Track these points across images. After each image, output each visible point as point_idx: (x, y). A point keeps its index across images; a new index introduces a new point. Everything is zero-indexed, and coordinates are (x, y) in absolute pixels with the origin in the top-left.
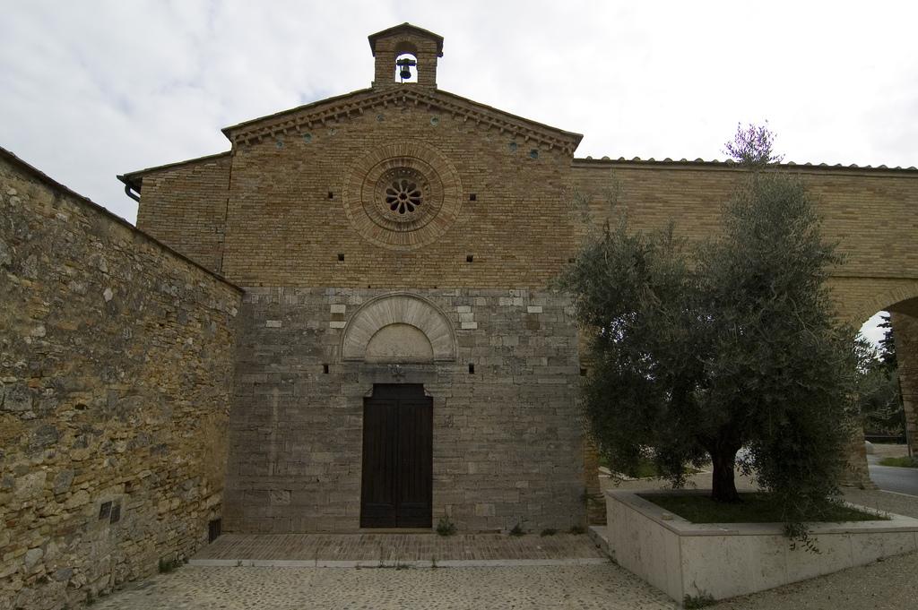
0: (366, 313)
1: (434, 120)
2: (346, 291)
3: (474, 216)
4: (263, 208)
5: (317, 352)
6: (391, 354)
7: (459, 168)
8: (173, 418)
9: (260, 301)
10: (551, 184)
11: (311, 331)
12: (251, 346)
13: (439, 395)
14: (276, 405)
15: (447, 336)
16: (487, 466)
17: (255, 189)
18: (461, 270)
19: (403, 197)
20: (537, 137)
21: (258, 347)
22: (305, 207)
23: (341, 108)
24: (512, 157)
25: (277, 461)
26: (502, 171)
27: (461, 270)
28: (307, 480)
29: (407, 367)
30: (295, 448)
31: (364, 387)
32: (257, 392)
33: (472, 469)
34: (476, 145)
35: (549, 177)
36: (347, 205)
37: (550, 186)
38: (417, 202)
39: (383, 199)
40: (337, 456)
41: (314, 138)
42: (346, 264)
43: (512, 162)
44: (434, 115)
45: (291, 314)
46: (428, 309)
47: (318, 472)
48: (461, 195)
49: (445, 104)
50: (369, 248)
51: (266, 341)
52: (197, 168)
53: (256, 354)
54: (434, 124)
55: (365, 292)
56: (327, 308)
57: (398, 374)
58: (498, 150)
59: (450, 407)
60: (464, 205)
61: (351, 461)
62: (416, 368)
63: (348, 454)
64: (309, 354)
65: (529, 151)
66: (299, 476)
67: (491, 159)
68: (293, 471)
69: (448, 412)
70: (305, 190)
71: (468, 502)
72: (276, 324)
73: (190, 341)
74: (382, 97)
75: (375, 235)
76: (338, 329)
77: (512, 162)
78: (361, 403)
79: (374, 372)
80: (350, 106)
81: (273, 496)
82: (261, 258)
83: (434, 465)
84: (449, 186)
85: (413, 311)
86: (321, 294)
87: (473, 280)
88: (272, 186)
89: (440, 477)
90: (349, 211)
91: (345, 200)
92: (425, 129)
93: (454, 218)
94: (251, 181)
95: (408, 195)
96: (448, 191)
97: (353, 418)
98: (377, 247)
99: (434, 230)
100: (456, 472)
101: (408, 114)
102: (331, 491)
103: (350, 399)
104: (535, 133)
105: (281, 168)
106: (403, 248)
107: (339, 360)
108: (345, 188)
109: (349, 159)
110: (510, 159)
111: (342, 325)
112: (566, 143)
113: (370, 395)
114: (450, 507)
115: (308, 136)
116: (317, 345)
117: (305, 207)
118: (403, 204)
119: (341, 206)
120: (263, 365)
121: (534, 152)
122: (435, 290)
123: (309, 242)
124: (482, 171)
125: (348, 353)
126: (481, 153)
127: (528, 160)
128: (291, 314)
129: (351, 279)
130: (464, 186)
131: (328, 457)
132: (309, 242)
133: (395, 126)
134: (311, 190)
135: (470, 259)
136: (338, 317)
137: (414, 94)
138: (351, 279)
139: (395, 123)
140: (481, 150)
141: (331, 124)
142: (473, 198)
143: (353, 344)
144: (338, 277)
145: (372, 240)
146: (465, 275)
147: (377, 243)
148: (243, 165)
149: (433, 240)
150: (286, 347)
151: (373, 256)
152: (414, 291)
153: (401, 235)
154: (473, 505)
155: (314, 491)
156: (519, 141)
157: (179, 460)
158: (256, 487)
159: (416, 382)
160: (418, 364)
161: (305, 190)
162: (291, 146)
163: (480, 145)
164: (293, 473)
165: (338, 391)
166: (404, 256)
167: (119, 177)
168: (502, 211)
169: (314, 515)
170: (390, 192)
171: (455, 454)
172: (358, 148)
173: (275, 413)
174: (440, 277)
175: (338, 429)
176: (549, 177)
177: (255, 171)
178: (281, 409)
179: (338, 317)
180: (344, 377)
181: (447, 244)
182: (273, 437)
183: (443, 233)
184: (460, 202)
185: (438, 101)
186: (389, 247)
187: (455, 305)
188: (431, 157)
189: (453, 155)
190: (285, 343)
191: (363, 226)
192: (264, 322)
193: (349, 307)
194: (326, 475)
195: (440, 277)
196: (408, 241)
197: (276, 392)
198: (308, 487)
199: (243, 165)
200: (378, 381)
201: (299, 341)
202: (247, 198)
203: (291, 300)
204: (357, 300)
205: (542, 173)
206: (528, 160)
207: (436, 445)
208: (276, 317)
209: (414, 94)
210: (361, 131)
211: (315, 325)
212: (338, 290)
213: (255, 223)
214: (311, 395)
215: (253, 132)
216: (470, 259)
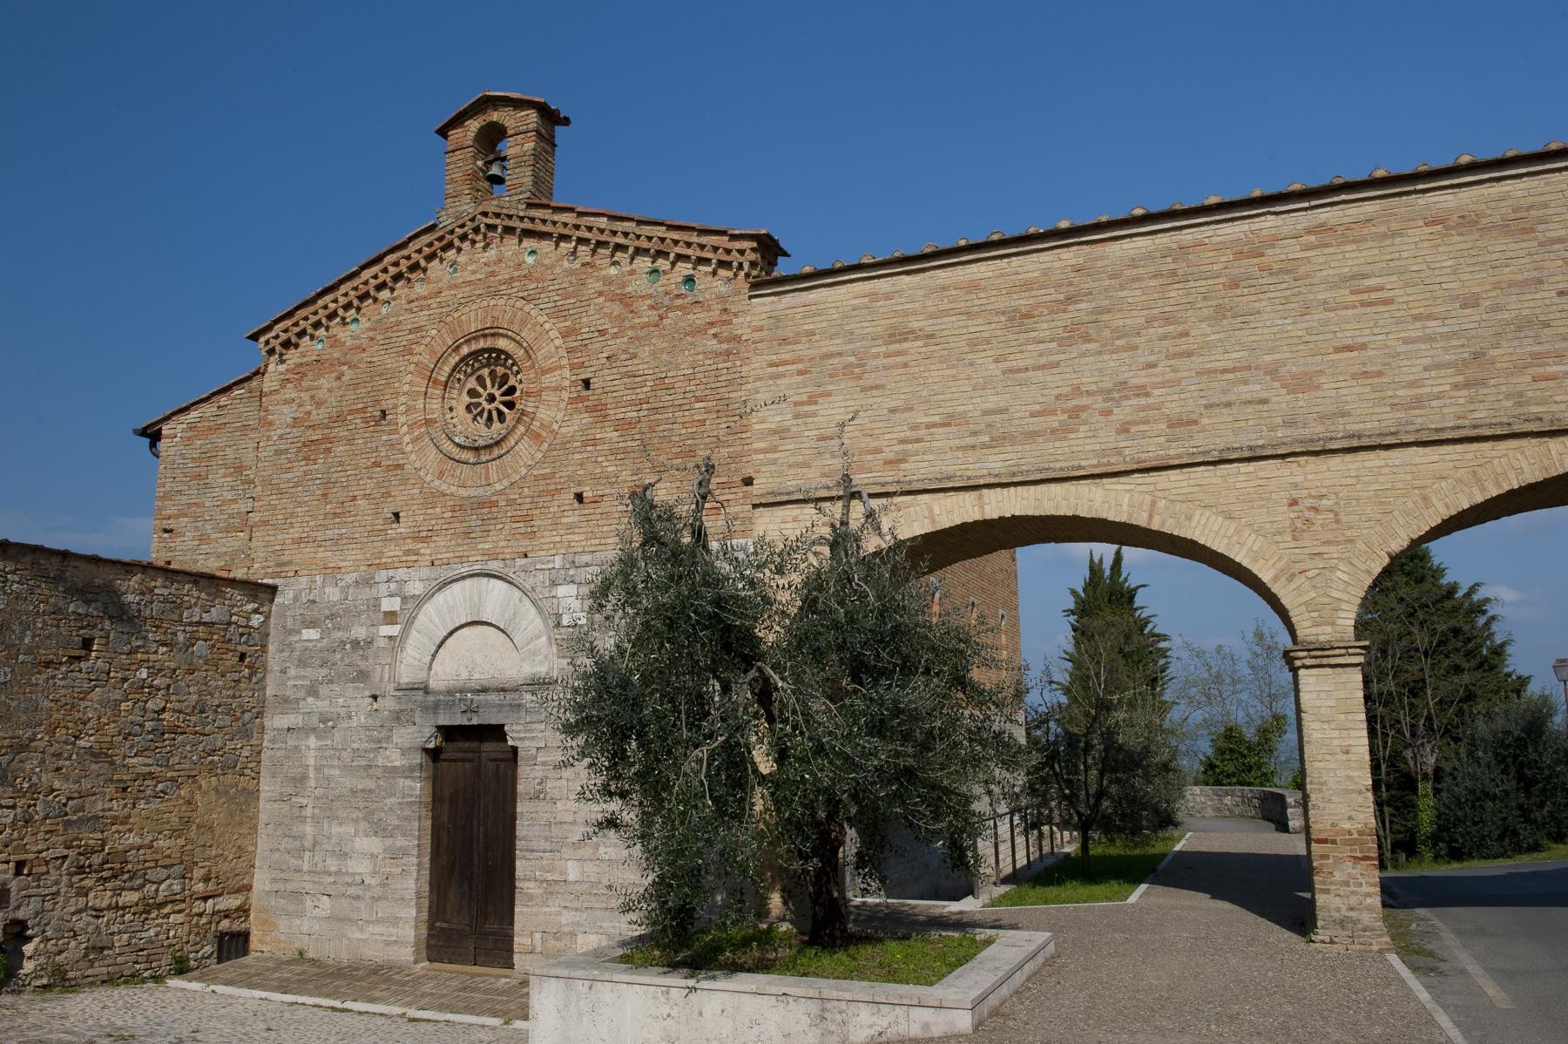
0: (429, 607)
1: (533, 252)
2: (401, 573)
3: (586, 419)
4: (299, 450)
5: (363, 676)
6: (464, 675)
7: (565, 335)
8: (112, 780)
9: (296, 599)
10: (715, 335)
11: (356, 644)
12: (284, 672)
13: (527, 743)
14: (311, 762)
15: (544, 639)
16: (595, 869)
17: (289, 420)
18: (564, 520)
19: (492, 399)
20: (689, 252)
21: (292, 672)
22: (350, 441)
23: (396, 264)
24: (650, 296)
25: (312, 850)
26: (632, 328)
27: (564, 520)
28: (349, 880)
29: (482, 697)
30: (336, 829)
31: (422, 733)
32: (291, 743)
33: (573, 872)
34: (594, 285)
35: (712, 324)
36: (405, 428)
37: (715, 341)
38: (510, 405)
39: (461, 409)
40: (389, 842)
41: (364, 323)
42: (403, 528)
43: (652, 307)
44: (529, 243)
45: (332, 617)
46: (517, 594)
47: (360, 867)
48: (567, 383)
49: (544, 221)
50: (432, 498)
51: (302, 663)
52: (223, 400)
53: (290, 683)
54: (530, 260)
55: (425, 572)
56: (377, 606)
57: (470, 710)
58: (629, 289)
59: (544, 764)
60: (572, 401)
61: (405, 853)
62: (493, 698)
63: (401, 842)
64: (353, 681)
65: (680, 279)
66: (339, 873)
67: (616, 308)
68: (332, 865)
69: (538, 772)
70: (351, 412)
71: (566, 929)
72: (311, 634)
73: (144, 674)
74: (452, 232)
75: (441, 475)
76: (390, 637)
77: (652, 307)
78: (418, 758)
79: (436, 707)
80: (408, 258)
81: (309, 904)
82: (296, 533)
83: (518, 863)
84: (550, 370)
85: (494, 597)
86: (368, 582)
87: (582, 537)
88: (309, 413)
89: (527, 884)
90: (407, 439)
91: (402, 419)
92: (517, 274)
93: (555, 426)
94: (286, 409)
95: (497, 394)
96: (548, 380)
97: (408, 782)
98: (445, 495)
99: (524, 453)
100: (549, 877)
101: (492, 253)
102: (380, 898)
103: (404, 752)
104: (689, 245)
105: (322, 381)
106: (480, 492)
107: (390, 688)
108: (403, 399)
109: (408, 351)
110: (648, 302)
111: (394, 630)
112: (742, 252)
113: (432, 745)
114: (538, 936)
115: (356, 320)
116: (363, 665)
117: (350, 441)
118: (490, 412)
119: (396, 431)
120: (297, 701)
121: (690, 280)
122: (524, 561)
123: (354, 498)
124: (602, 333)
125: (406, 676)
126: (601, 300)
127: (678, 296)
128: (332, 617)
129: (408, 552)
130: (573, 367)
131: (374, 845)
132: (354, 498)
133: (473, 278)
134: (357, 411)
135: (579, 497)
136: (391, 617)
137: (498, 215)
138: (408, 552)
139: (474, 272)
140: (601, 294)
141: (385, 294)
142: (587, 384)
143: (410, 664)
144: (393, 551)
145: (437, 483)
146: (570, 528)
147: (443, 487)
148: (275, 385)
149: (524, 471)
150: (324, 671)
151: (438, 510)
152: (494, 566)
153: (478, 468)
154: (573, 934)
155: (358, 897)
156: (663, 264)
157: (132, 839)
158: (290, 887)
159: (493, 722)
160: (503, 690)
161: (351, 412)
162: (335, 343)
163: (598, 286)
164: (333, 869)
165: (388, 739)
166: (481, 504)
167: (135, 431)
168: (632, 403)
169: (358, 935)
170: (472, 393)
171: (548, 846)
172: (420, 329)
173: (312, 774)
174: (532, 535)
175: (389, 801)
176: (712, 324)
177: (290, 392)
178: (318, 769)
179: (391, 617)
180: (397, 717)
181: (544, 477)
182: (309, 812)
183: (539, 455)
184: (565, 395)
185: (532, 220)
186: (462, 492)
187: (554, 584)
188: (523, 322)
189: (558, 313)
190: (323, 664)
191: (423, 460)
192: (299, 632)
193: (404, 599)
194: (374, 873)
195: (532, 535)
196: (487, 478)
197: (312, 741)
198: (352, 891)
199: (275, 385)
200: (444, 720)
201: (342, 659)
202: (281, 437)
203: (333, 594)
204: (416, 588)
205: (699, 317)
206: (678, 296)
207: (522, 829)
208: (312, 624)
209: (498, 215)
210: (425, 298)
211: (360, 632)
212: (391, 573)
213: (289, 475)
214: (355, 746)
215: (286, 331)
216: (579, 497)
